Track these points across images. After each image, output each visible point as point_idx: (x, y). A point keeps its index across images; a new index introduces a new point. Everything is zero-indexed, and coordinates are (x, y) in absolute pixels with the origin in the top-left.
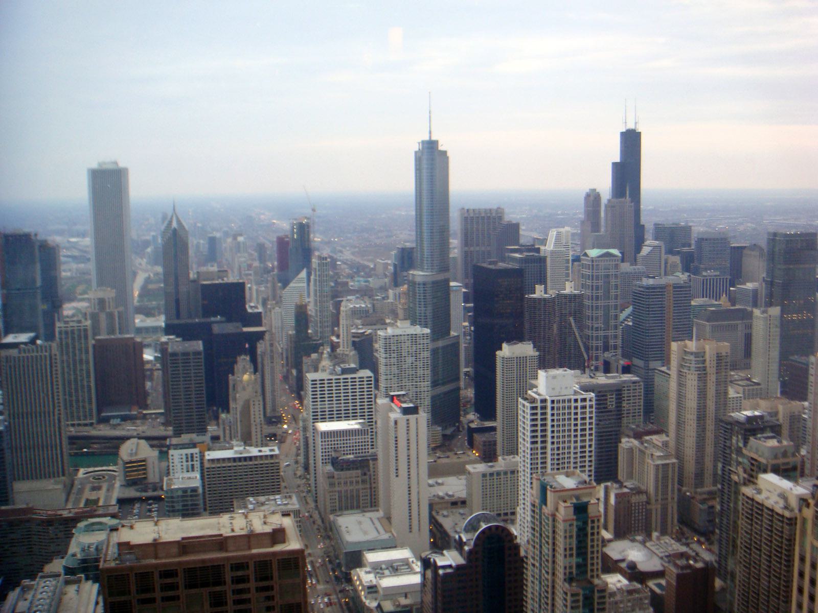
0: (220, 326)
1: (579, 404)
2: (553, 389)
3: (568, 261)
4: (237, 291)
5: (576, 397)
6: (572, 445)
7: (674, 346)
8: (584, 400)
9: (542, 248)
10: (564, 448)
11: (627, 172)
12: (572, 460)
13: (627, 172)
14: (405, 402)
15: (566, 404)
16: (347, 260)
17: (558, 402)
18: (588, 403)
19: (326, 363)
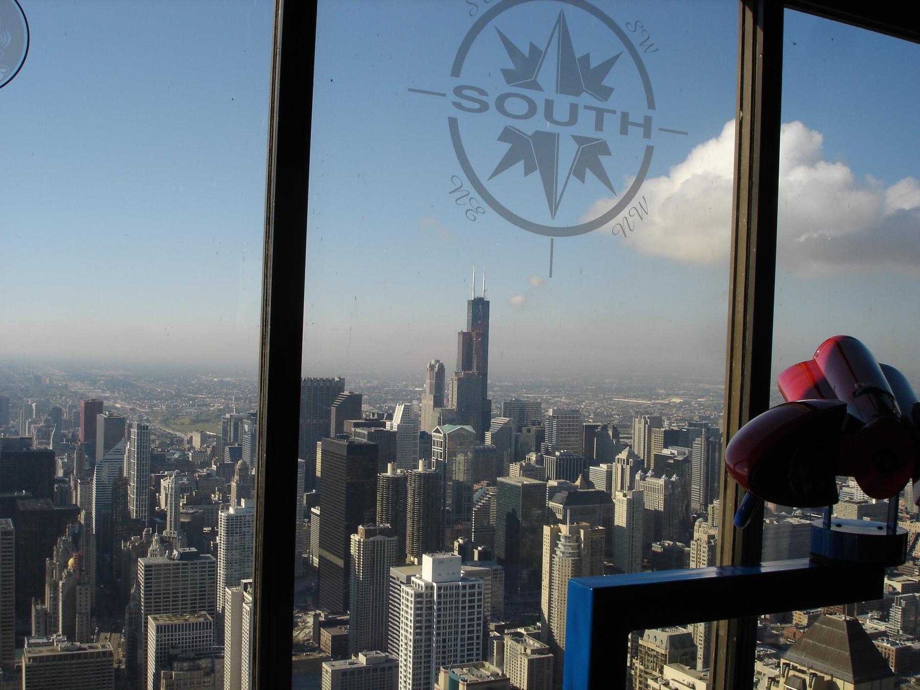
1: (468, 591)
3: (415, 438)
4: (48, 458)
6: (459, 636)
7: (547, 530)
8: (473, 587)
9: (388, 423)
11: (475, 343)
13: (475, 343)
15: (454, 591)
16: (155, 429)
17: (446, 589)
18: (476, 590)
19: (154, 546)
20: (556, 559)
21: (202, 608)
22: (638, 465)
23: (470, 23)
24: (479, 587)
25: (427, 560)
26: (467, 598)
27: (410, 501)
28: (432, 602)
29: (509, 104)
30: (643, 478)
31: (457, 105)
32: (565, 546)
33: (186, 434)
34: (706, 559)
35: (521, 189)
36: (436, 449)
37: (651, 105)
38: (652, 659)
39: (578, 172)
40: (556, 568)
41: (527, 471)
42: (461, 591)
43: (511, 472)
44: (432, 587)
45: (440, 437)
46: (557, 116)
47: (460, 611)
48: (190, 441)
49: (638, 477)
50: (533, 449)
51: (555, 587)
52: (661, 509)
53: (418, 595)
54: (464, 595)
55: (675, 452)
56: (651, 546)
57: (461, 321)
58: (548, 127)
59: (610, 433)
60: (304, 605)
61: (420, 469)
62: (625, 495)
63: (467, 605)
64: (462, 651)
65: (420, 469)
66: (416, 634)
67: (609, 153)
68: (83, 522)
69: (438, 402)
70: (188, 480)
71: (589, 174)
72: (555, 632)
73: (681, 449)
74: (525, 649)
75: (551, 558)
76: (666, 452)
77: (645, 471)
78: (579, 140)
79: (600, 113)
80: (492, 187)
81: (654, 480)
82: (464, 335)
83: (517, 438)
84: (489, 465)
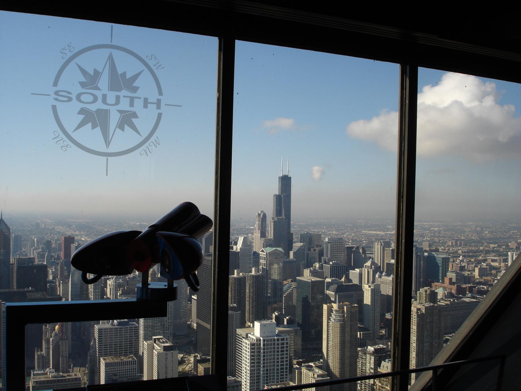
1: (280, 342)
2: (264, 333)
4: (43, 269)
6: (276, 368)
7: (325, 307)
8: (283, 339)
9: (235, 247)
10: (270, 370)
11: (283, 201)
12: (276, 378)
13: (283, 201)
14: (163, 342)
15: (272, 342)
17: (268, 341)
18: (285, 341)
20: (331, 323)
21: (131, 353)
23: (63, 61)
24: (286, 340)
25: (257, 324)
26: (280, 346)
27: (247, 291)
28: (260, 348)
29: (83, 98)
30: (380, 277)
31: (56, 99)
32: (335, 316)
35: (91, 136)
36: (262, 261)
37: (161, 93)
39: (121, 126)
40: (330, 328)
41: (314, 273)
42: (276, 342)
43: (305, 273)
44: (260, 340)
45: (264, 255)
46: (109, 101)
47: (276, 353)
49: (377, 276)
50: (317, 260)
51: (330, 339)
53: (252, 345)
54: (278, 344)
56: (385, 315)
57: (275, 189)
58: (105, 107)
59: (361, 251)
60: (188, 350)
61: (253, 273)
62: (370, 287)
63: (280, 350)
64: (278, 376)
65: (253, 273)
66: (251, 367)
67: (137, 117)
69: (263, 234)
70: (122, 280)
71: (126, 127)
72: (331, 364)
74: (314, 374)
75: (328, 323)
77: (381, 273)
78: (120, 112)
79: (132, 100)
80: (74, 135)
81: (386, 278)
83: (308, 254)
84: (292, 270)
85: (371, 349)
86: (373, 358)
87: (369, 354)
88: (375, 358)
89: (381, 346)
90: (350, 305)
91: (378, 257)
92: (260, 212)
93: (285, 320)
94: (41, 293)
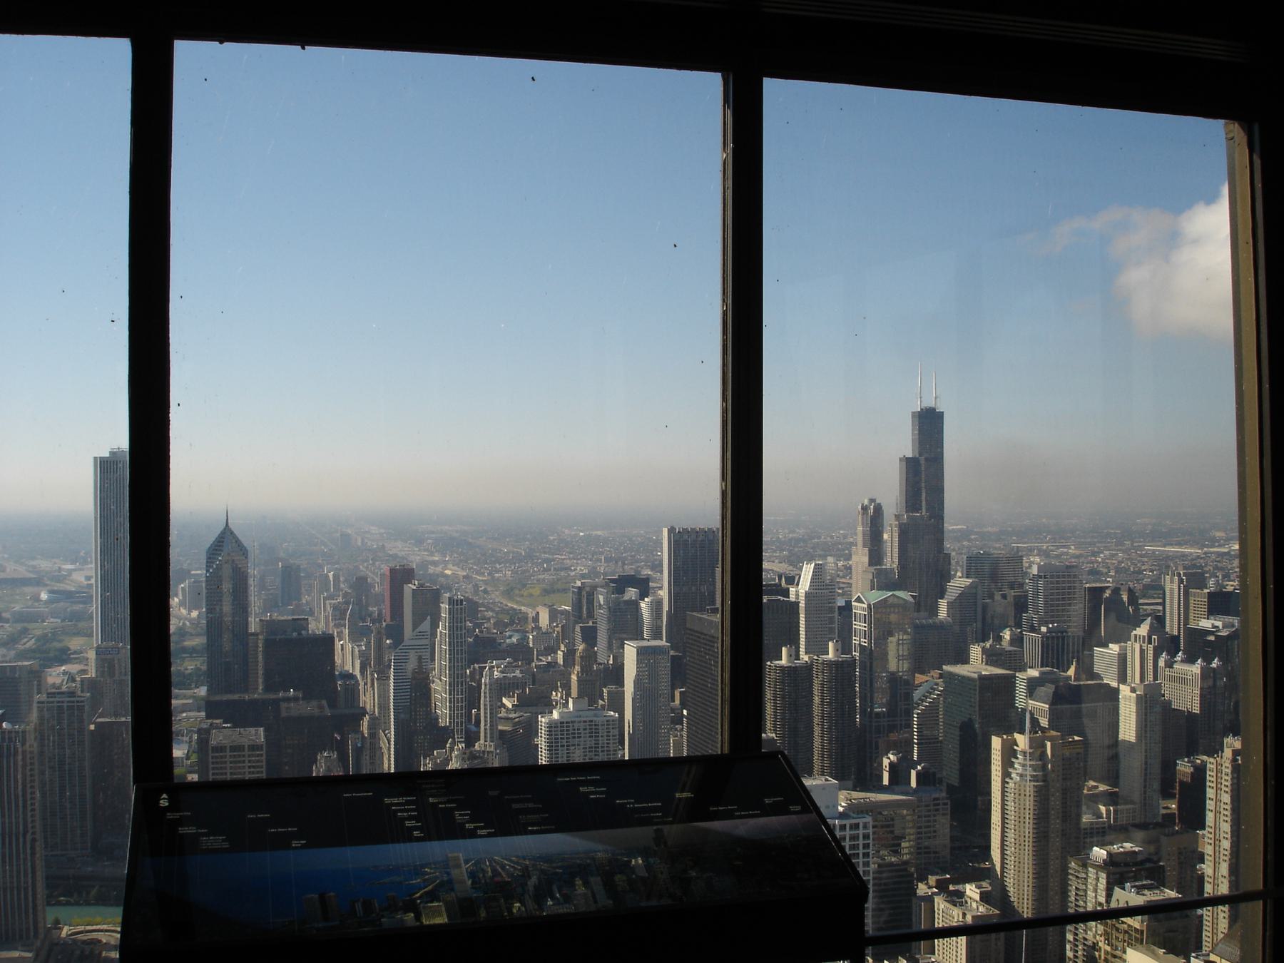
0: (294, 703)
3: (831, 610)
5: (844, 822)
7: (996, 742)
8: (856, 826)
9: (792, 590)
16: (494, 603)
18: (861, 832)
20: (1011, 785)
22: (1169, 645)
24: (865, 827)
27: (817, 699)
30: (1170, 665)
32: (1024, 766)
33: (533, 606)
34: (1228, 784)
36: (858, 626)
38: (1121, 936)
40: (1010, 797)
41: (992, 657)
48: (536, 619)
49: (1161, 663)
52: (1196, 710)
55: (1219, 624)
56: (1176, 764)
59: (1125, 598)
61: (831, 655)
62: (1133, 690)
65: (831, 655)
68: (366, 732)
69: (876, 556)
73: (1229, 619)
74: (964, 915)
75: (1004, 783)
76: (1206, 624)
77: (1173, 654)
81: (1185, 667)
82: (908, 460)
83: (985, 607)
84: (937, 647)
85: (1099, 853)
86: (1103, 876)
87: (1094, 866)
88: (1108, 878)
89: (1128, 846)
90: (1062, 737)
91: (1172, 614)
92: (866, 502)
93: (913, 773)
94: (315, 703)
